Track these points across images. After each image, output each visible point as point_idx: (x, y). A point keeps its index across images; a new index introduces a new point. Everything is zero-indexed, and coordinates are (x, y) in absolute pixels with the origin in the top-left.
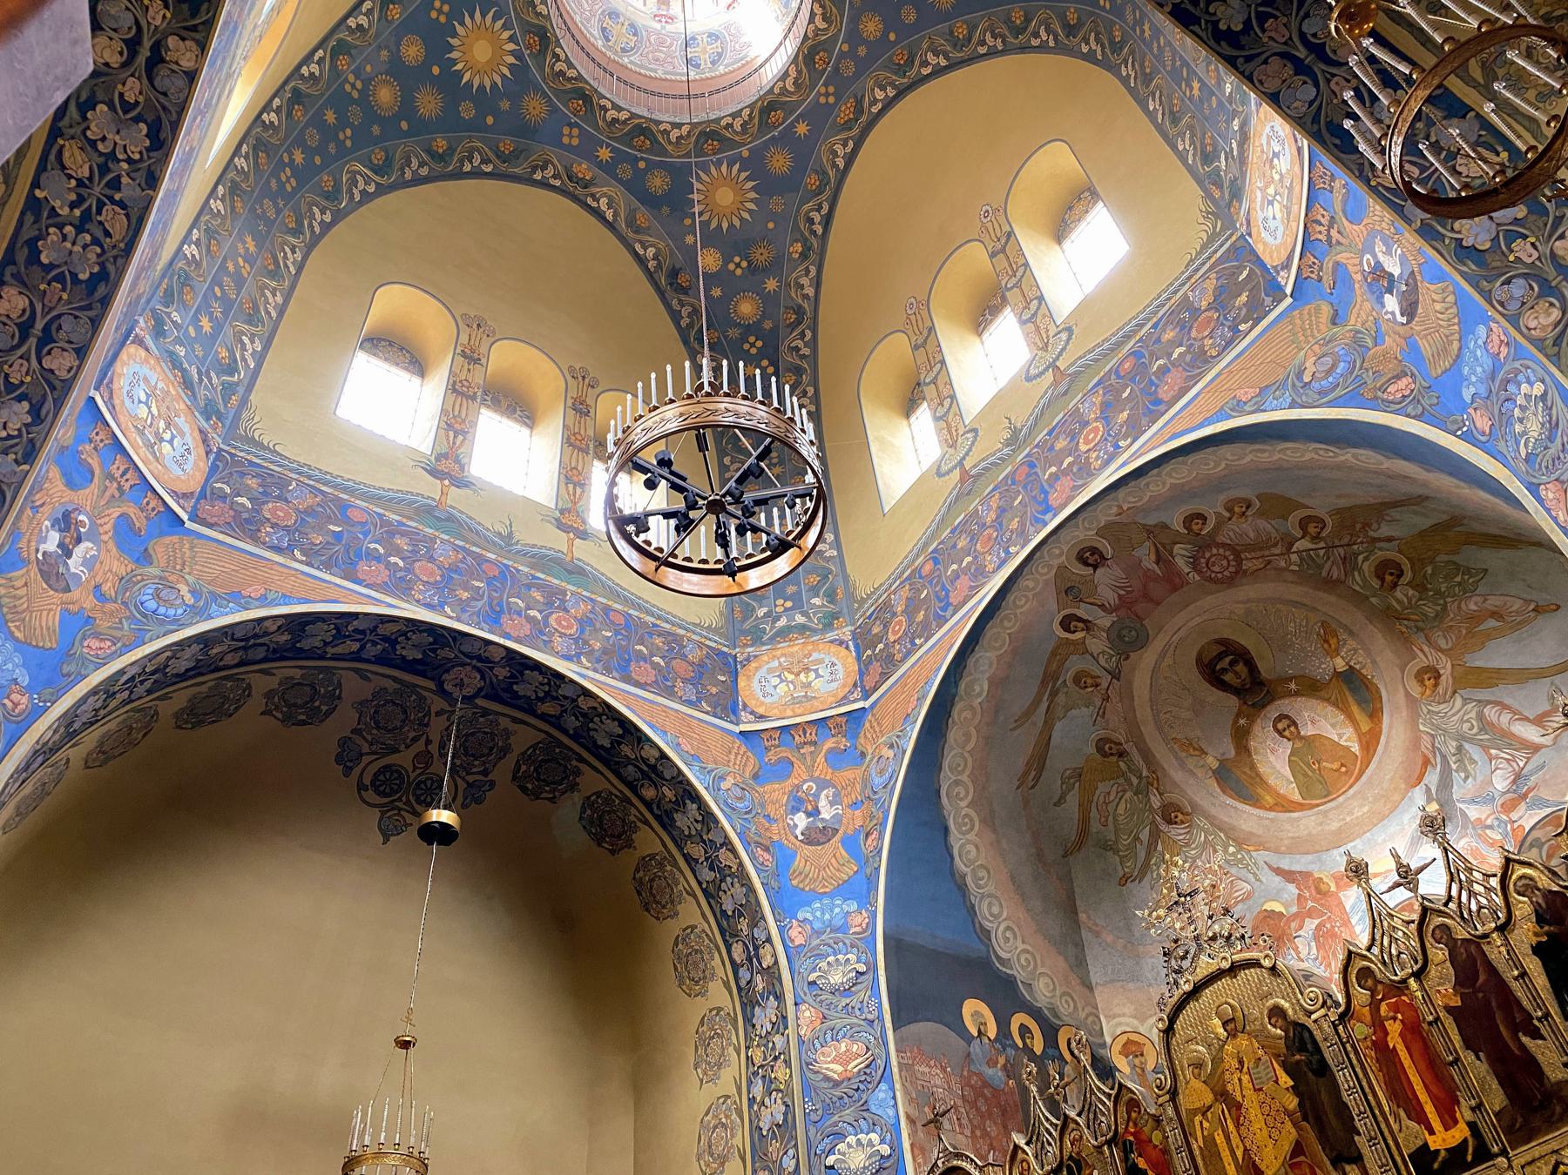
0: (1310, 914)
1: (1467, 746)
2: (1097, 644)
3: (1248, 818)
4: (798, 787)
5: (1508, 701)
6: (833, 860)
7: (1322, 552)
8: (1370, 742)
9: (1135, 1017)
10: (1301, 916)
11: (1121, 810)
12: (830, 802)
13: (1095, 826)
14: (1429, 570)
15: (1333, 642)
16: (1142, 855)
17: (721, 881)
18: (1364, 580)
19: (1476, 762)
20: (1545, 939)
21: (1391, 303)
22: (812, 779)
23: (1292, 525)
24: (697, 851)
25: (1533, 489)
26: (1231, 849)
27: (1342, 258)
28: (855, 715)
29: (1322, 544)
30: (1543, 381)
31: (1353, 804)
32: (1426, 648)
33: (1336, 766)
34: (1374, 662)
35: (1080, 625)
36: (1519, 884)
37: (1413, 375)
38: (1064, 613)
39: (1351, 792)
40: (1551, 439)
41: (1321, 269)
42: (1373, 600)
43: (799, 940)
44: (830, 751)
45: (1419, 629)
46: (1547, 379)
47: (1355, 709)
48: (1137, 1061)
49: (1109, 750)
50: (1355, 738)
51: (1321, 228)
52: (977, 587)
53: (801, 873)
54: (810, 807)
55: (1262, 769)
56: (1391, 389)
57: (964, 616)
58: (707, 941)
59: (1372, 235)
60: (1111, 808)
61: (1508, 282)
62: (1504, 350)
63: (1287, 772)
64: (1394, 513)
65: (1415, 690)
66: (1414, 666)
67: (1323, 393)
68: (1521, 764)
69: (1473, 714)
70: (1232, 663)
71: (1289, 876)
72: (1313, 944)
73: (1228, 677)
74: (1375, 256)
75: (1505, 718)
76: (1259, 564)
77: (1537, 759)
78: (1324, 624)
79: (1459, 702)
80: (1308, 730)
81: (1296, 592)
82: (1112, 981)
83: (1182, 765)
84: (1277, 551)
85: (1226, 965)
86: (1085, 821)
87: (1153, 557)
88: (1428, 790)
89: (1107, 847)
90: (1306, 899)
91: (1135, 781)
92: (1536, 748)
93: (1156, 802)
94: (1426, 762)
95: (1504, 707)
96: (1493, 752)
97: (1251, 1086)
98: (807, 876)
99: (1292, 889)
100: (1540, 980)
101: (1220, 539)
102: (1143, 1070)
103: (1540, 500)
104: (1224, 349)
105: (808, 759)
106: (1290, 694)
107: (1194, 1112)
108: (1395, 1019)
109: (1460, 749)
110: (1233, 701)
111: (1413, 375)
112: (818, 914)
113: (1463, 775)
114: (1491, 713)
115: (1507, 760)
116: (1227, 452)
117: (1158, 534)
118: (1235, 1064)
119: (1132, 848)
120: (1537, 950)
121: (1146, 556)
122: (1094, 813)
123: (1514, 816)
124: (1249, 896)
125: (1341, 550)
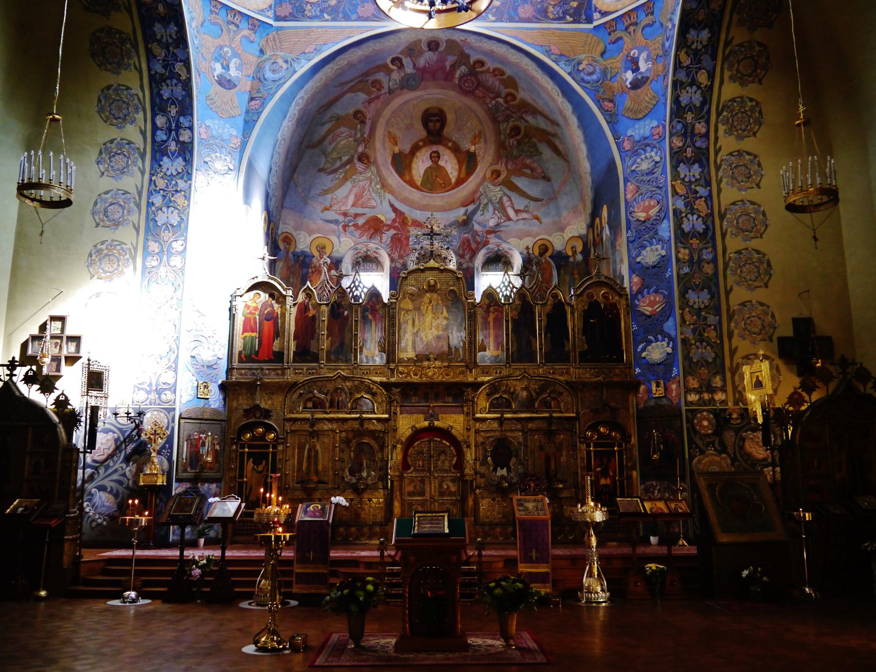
0: (395, 228)
1: (490, 204)
2: (396, 76)
3: (393, 178)
4: (221, 48)
5: (513, 199)
6: (230, 102)
7: (503, 108)
8: (460, 182)
9: (293, 228)
10: (390, 227)
11: (343, 143)
12: (236, 67)
13: (326, 142)
14: (527, 140)
15: (477, 140)
16: (338, 164)
17: (168, 78)
18: (506, 127)
21: (629, 76)
22: (230, 47)
23: (504, 91)
24: (160, 53)
25: (626, 180)
26: (378, 186)
27: (627, 39)
28: (266, 26)
29: (506, 105)
30: (661, 158)
31: (438, 199)
32: (503, 164)
33: (441, 182)
34: (483, 157)
35: (399, 64)
37: (615, 105)
38: (401, 56)
39: (440, 195)
40: (647, 174)
41: (614, 31)
42: (502, 136)
43: (204, 136)
44: (244, 36)
45: (507, 157)
46: (663, 160)
47: (464, 168)
48: (287, 246)
49: (359, 116)
50: (456, 177)
51: (629, 20)
52: (377, 17)
53: (212, 99)
54: (225, 63)
55: (414, 165)
56: (606, 103)
57: (360, 27)
58: (136, 101)
59: (646, 48)
60: (339, 139)
61: (679, 122)
62: (657, 137)
63: (422, 172)
64: (539, 117)
65: (488, 175)
66: (495, 167)
67: (583, 80)
69: (499, 196)
70: (437, 121)
71: (395, 209)
72: (390, 239)
73: (431, 125)
74: (639, 54)
75: (508, 204)
76: (481, 94)
77: (507, 223)
78: (480, 132)
79: (498, 188)
80: (441, 163)
81: (482, 114)
82: (291, 209)
83: (384, 143)
84: (491, 95)
85: (442, 268)
86: (324, 138)
87: (452, 63)
88: (467, 210)
89: (324, 153)
90: (396, 222)
91: (359, 135)
92: (509, 219)
93: (360, 149)
94: (473, 202)
95: (510, 200)
96: (496, 212)
98: (215, 103)
99: (393, 215)
101: (480, 77)
103: (625, 186)
104: (555, 20)
105: (232, 34)
106: (446, 146)
107: (403, 310)
108: (494, 313)
109: (487, 204)
110: (424, 133)
111: (615, 105)
112: (216, 127)
114: (505, 199)
116: (526, 61)
117: (463, 58)
118: (428, 301)
119: (335, 160)
120: (548, 315)
121: (450, 60)
122: (330, 137)
123: (489, 236)
124: (373, 207)
125: (509, 112)
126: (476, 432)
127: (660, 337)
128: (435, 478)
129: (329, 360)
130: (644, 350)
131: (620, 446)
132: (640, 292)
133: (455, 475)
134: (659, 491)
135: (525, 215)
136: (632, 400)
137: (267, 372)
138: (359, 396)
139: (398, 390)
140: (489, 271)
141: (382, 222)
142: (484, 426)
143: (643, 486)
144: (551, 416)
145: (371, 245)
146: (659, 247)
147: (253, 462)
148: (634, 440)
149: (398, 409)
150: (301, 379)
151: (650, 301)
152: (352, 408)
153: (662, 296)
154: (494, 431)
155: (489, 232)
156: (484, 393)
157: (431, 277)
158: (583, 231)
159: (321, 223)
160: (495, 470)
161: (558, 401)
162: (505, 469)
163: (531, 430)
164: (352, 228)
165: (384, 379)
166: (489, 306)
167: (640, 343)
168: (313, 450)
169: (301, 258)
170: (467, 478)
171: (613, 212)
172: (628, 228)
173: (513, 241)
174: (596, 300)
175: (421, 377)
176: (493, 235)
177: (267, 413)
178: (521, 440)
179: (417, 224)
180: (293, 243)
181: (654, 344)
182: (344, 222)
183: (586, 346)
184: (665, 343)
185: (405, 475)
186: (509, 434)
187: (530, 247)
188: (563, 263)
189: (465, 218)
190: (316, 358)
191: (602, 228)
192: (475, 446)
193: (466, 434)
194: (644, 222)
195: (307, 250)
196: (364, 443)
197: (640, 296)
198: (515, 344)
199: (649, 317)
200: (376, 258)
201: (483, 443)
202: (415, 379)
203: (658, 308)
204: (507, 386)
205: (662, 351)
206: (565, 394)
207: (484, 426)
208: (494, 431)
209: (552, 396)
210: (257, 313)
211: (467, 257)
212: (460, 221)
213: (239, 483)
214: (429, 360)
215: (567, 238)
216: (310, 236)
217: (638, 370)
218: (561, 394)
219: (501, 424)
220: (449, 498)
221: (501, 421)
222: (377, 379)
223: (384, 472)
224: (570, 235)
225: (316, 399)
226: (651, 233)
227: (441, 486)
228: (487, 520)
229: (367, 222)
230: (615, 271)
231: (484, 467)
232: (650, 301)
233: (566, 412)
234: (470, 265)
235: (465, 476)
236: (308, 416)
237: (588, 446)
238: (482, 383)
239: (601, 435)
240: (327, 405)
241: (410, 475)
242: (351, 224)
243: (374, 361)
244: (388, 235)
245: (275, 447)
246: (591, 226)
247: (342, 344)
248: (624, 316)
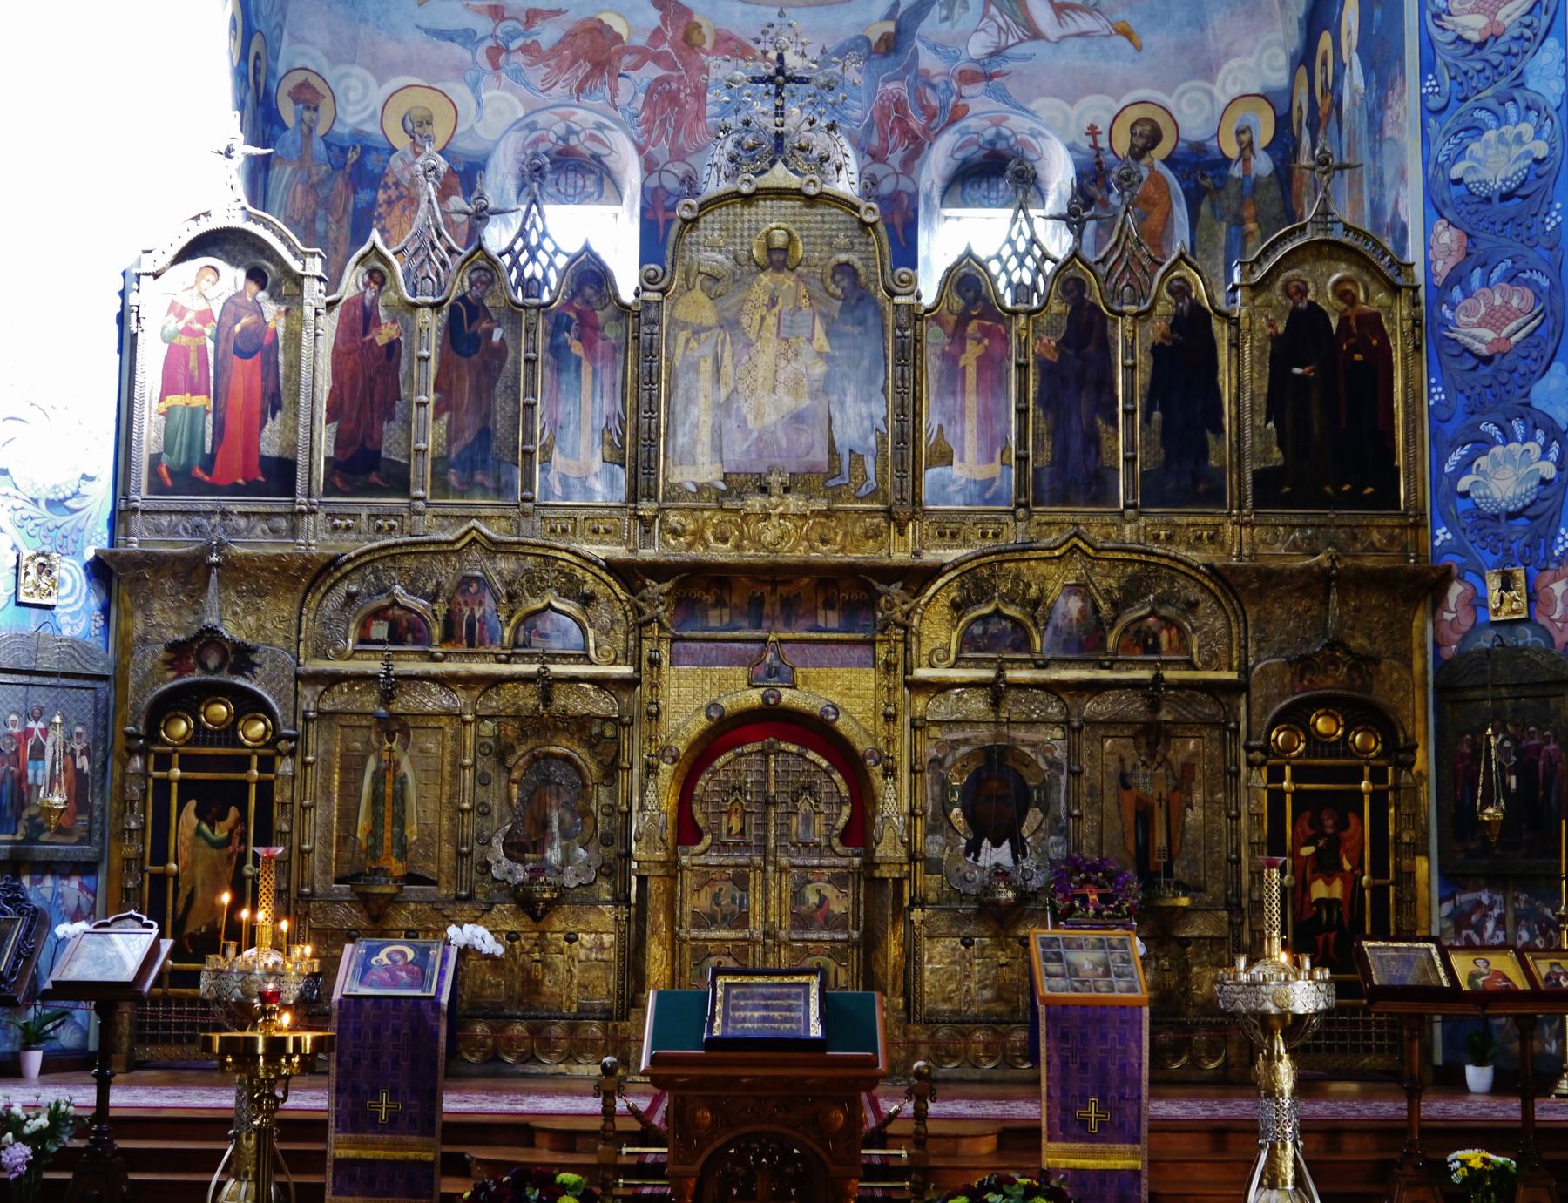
0: (658, 59)
9: (326, 54)
10: (644, 55)
19: (967, 8)
20: (1168, 344)
36: (1176, 283)
48: (307, 115)
68: (1011, 41)
72: (642, 96)
77: (1028, 47)
85: (812, 191)
90: (664, 39)
92: (1036, 35)
96: (993, 10)
97: (774, 330)
100: (1142, 378)
102: (311, 130)
107: (685, 325)
108: (979, 342)
113: (944, 13)
115: (1000, 28)
118: (764, 298)
120: (1157, 351)
123: (966, 90)
126: (913, 727)
127: (1518, 427)
128: (782, 870)
129: (441, 485)
130: (1465, 467)
131: (1378, 775)
132: (1457, 277)
133: (844, 862)
134: (1500, 922)
135: (1085, 23)
136: (1422, 627)
137: (243, 523)
138: (538, 604)
139: (665, 587)
140: (965, 204)
141: (618, 37)
142: (941, 708)
143: (1447, 908)
144: (1158, 678)
145: (580, 114)
146: (1527, 129)
147: (199, 813)
148: (1424, 760)
149: (665, 647)
150: (351, 546)
151: (1491, 308)
152: (516, 645)
153: (1529, 293)
154: (974, 723)
155: (967, 77)
156: (944, 600)
157: (774, 220)
158: (1278, 77)
159: (416, 40)
160: (974, 848)
161: (1180, 629)
162: (1006, 846)
163: (1092, 722)
164: (520, 58)
165: (620, 552)
166: (963, 319)
167: (1453, 446)
168: (389, 776)
169: (352, 157)
170: (885, 872)
171: (1377, 14)
172: (1427, 67)
173: (1045, 106)
174: (1312, 305)
175: (738, 547)
176: (979, 88)
177: (242, 657)
178: (1060, 754)
179: (731, 46)
180: (325, 107)
181: (1497, 450)
182: (494, 36)
183: (1277, 454)
184: (1534, 448)
185: (685, 860)
186: (1020, 734)
187: (1103, 127)
188: (1207, 183)
189: (890, 27)
190: (398, 482)
191: (1340, 67)
192: (912, 770)
193: (882, 732)
194: (1480, 45)
195: (371, 128)
196: (553, 756)
197: (1457, 293)
198: (1048, 444)
199: (1487, 360)
200: (596, 157)
201: (937, 762)
202: (721, 553)
203: (1515, 331)
204: (1017, 578)
205: (1524, 471)
206: (1206, 607)
207: (941, 708)
208: (974, 723)
209: (1163, 612)
210: (208, 331)
211: (895, 158)
212: (875, 38)
213: (153, 876)
214: (764, 490)
215: (1224, 100)
216: (381, 83)
217: (1443, 534)
218: (1192, 606)
219: (996, 702)
220: (825, 935)
221: (996, 691)
222: (599, 551)
223: (617, 848)
224: (1235, 91)
225: (398, 612)
226: (1503, 83)
227: (798, 896)
228: (946, 1007)
229: (570, 37)
230: (1377, 211)
231: (939, 839)
232: (1491, 308)
233: (1207, 665)
234: (904, 183)
235: (876, 866)
236: (374, 666)
237: (1276, 775)
238: (936, 571)
239: (1317, 743)
240: (437, 631)
241: (702, 860)
242: (515, 44)
243: (587, 491)
244: (634, 84)
245: (267, 764)
246: (1305, 58)
247: (485, 434)
248: (1405, 358)
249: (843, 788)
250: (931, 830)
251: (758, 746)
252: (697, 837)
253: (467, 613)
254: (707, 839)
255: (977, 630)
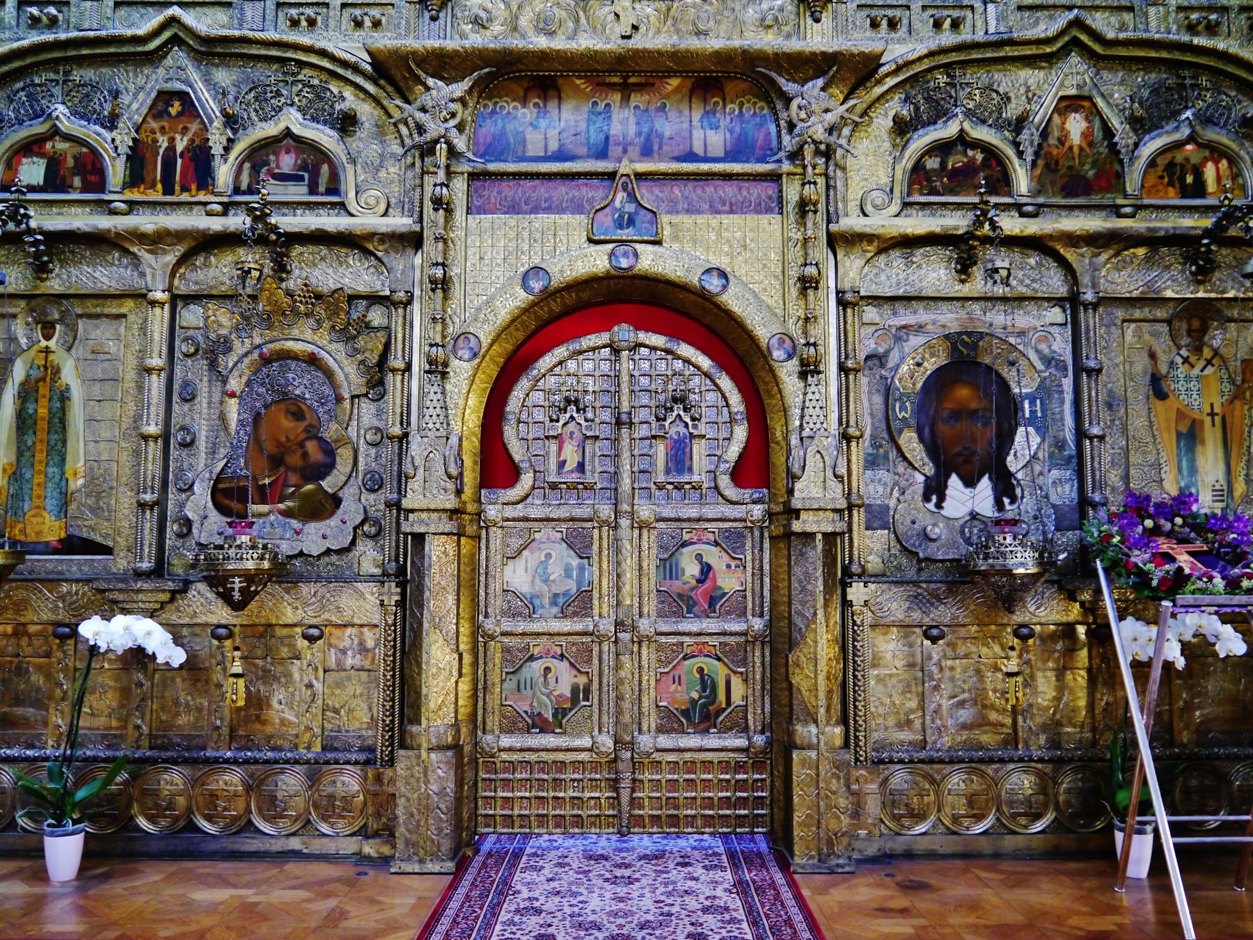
126: (842, 303)
128: (642, 526)
133: (737, 512)
138: (271, 129)
139: (459, 89)
149: (460, 185)
152: (237, 191)
160: (935, 489)
161: (1233, 161)
162: (985, 484)
168: (44, 390)
185: (492, 512)
192: (842, 368)
193: (796, 310)
196: (285, 356)
201: (876, 359)
209: (1211, 134)
220: (711, 625)
223: (388, 494)
225: (61, 146)
227: (668, 566)
228: (905, 736)
231: (882, 474)
235: (796, 513)
240: (116, 171)
241: (519, 511)
249: (735, 399)
250: (872, 463)
251: (604, 338)
252: (511, 474)
253: (163, 143)
254: (526, 480)
255: (932, 163)
